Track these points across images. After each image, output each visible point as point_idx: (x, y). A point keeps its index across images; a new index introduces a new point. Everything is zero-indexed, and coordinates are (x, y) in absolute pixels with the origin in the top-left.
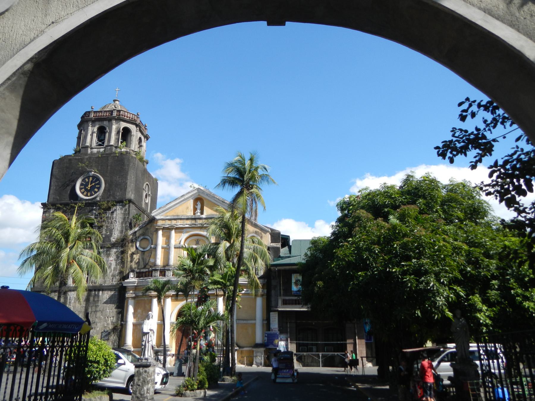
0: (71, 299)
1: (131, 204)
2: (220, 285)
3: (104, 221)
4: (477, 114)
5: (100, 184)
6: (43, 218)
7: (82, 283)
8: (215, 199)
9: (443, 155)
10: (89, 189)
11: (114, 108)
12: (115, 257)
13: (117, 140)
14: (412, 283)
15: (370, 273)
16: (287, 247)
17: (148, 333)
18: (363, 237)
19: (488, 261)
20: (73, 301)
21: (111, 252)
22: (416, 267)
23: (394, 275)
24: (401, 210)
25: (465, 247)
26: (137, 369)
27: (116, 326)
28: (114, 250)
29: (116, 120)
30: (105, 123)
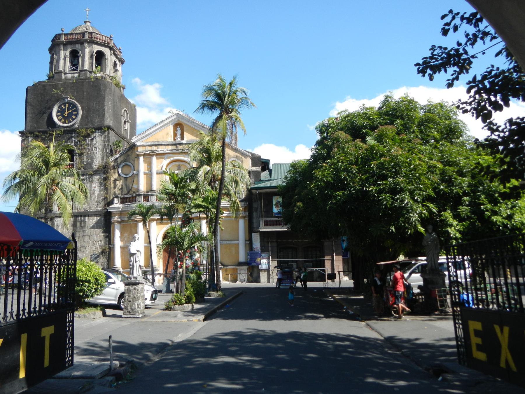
1: (110, 131)
2: (203, 208)
3: (84, 148)
4: (460, 27)
5: (77, 110)
6: (22, 146)
7: (67, 209)
9: (422, 72)
10: (66, 116)
11: (86, 30)
12: (98, 184)
13: (91, 65)
14: (388, 201)
15: (347, 192)
16: (267, 170)
17: (136, 254)
18: (341, 158)
19: (461, 179)
21: (94, 179)
22: (391, 185)
23: (371, 194)
24: (379, 130)
25: (440, 166)
26: (127, 287)
27: (105, 250)
28: (96, 177)
29: (88, 43)
30: (78, 47)
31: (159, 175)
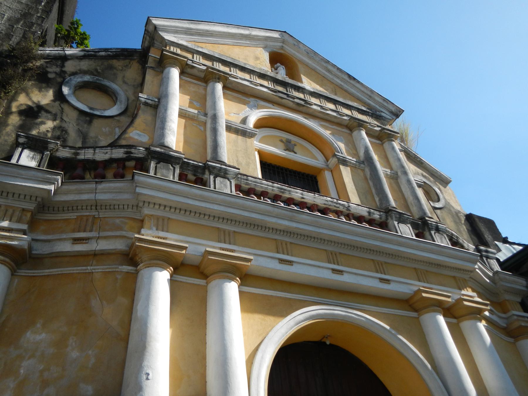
8: (330, 67)
31: (233, 136)
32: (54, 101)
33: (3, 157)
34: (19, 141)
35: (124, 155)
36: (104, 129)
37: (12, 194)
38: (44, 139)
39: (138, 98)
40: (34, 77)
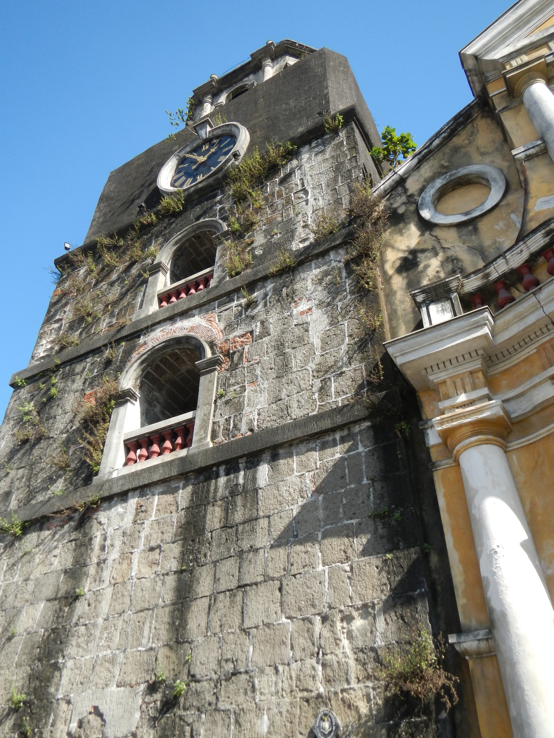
0: (108, 542)
12: (320, 294)
20: (114, 555)
32: (422, 235)
33: (413, 328)
34: (418, 301)
35: (545, 239)
36: (497, 227)
37: (449, 362)
38: (441, 282)
39: (514, 159)
40: (387, 224)
